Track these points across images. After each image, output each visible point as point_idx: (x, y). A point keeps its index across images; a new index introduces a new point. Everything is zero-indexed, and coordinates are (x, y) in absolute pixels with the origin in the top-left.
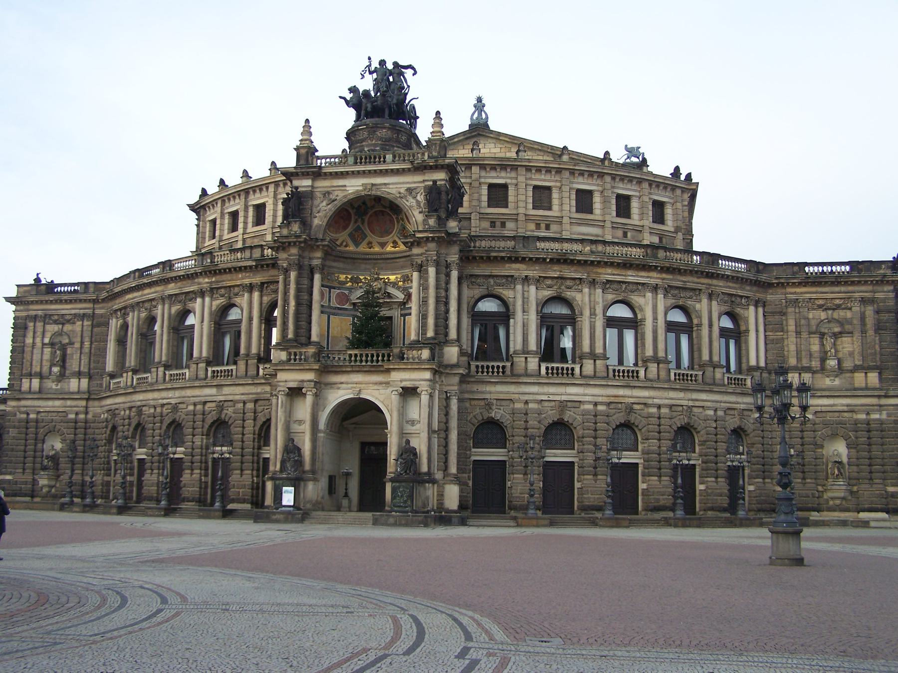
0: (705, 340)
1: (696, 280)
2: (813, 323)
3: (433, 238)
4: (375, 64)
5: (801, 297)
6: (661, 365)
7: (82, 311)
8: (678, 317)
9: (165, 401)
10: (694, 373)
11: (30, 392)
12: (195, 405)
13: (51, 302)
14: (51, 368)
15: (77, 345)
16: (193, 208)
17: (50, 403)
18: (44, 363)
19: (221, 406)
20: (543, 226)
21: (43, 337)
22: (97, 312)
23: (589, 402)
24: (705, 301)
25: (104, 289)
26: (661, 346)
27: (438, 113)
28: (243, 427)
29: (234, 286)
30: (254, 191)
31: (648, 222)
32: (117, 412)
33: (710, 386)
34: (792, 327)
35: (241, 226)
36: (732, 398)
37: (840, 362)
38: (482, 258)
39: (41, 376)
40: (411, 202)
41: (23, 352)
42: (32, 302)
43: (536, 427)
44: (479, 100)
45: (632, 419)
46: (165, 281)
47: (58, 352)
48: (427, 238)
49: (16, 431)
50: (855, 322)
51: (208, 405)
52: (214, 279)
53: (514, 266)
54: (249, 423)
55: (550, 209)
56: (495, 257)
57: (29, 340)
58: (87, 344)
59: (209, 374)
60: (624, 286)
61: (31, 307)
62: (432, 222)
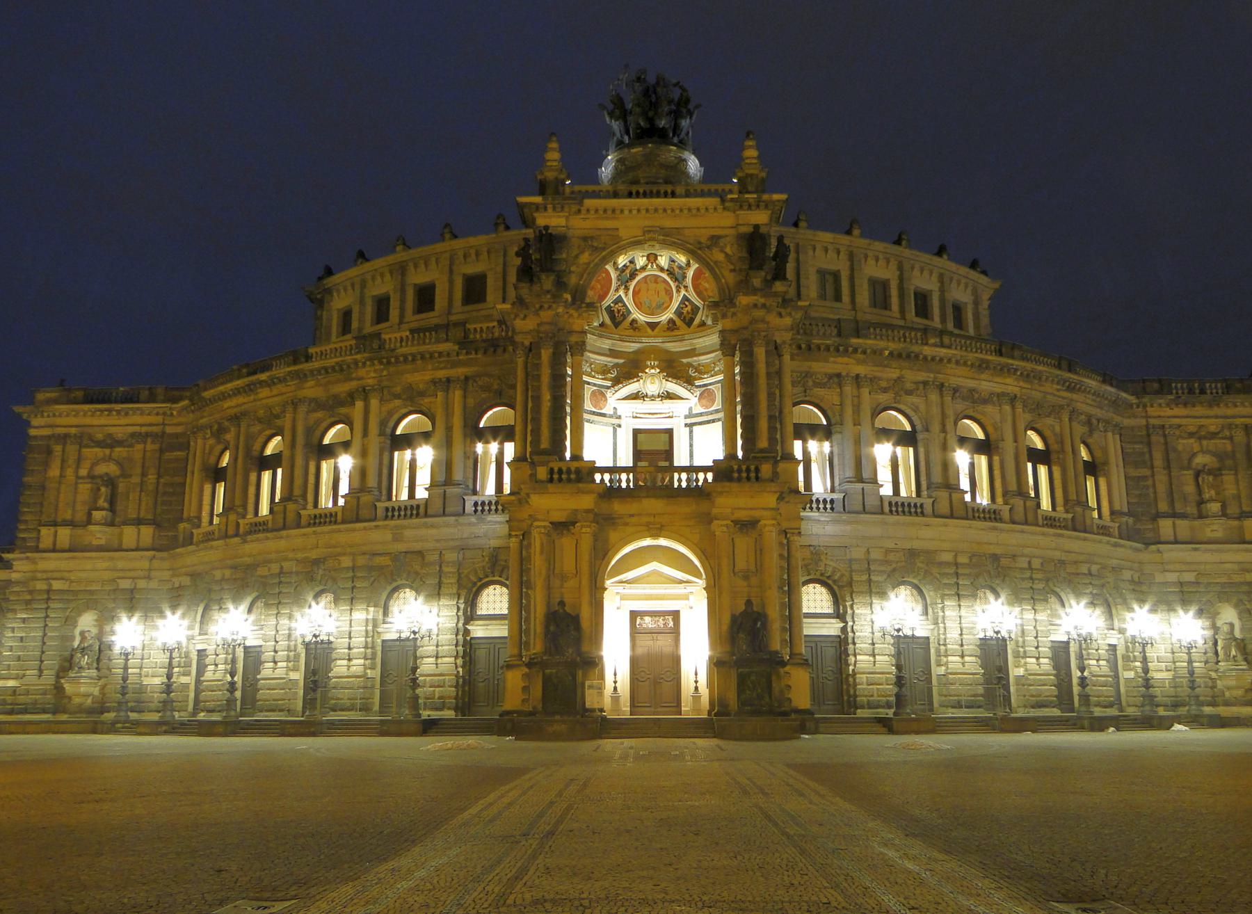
3: (764, 306)
6: (1029, 504)
7: (144, 429)
11: (54, 550)
14: (90, 515)
15: (136, 480)
18: (78, 507)
21: (78, 467)
22: (169, 430)
30: (416, 266)
34: (1158, 461)
35: (394, 314)
37: (1224, 507)
39: (71, 524)
40: (720, 257)
41: (43, 488)
47: (103, 489)
50: (1239, 456)
53: (840, 360)
57: (54, 472)
62: (757, 282)
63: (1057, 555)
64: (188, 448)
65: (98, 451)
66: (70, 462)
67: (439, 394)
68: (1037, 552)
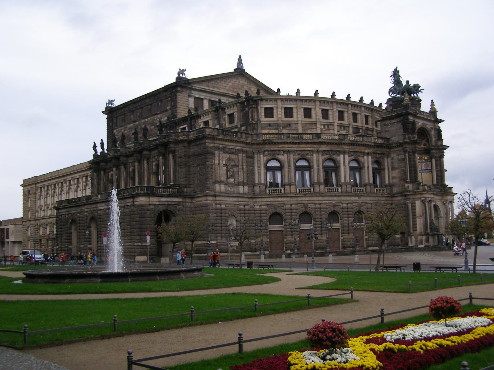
9: (327, 202)
15: (240, 167)
17: (231, 199)
19: (360, 205)
22: (248, 150)
25: (248, 138)
27: (432, 101)
29: (357, 152)
32: (279, 205)
42: (219, 139)
44: (240, 57)
47: (232, 170)
49: (215, 215)
52: (350, 147)
57: (217, 162)
61: (216, 142)
64: (253, 158)
66: (221, 158)
67: (366, 157)
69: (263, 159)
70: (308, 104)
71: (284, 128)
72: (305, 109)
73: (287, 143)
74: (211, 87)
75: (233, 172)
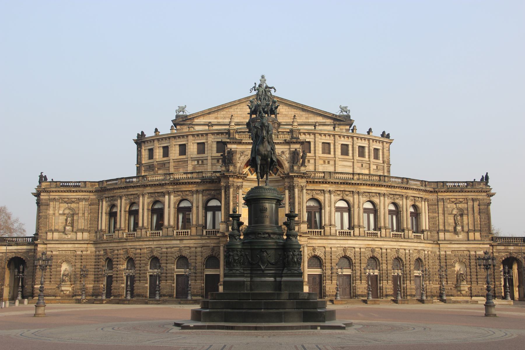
0: (405, 218)
1: (401, 191)
2: (450, 209)
4: (257, 86)
5: (444, 198)
7: (82, 197)
8: (392, 208)
9: (147, 246)
10: (400, 233)
11: (53, 240)
12: (167, 248)
13: (65, 192)
16: (136, 142)
17: (65, 246)
18: (60, 224)
20: (326, 162)
22: (91, 197)
23: (357, 247)
24: (405, 200)
26: (387, 221)
28: (196, 260)
29: (186, 191)
31: (372, 159)
33: (406, 239)
34: (441, 211)
36: (416, 245)
37: (463, 227)
38: (310, 182)
39: (57, 231)
42: (53, 191)
43: (335, 260)
44: (263, 77)
45: (375, 254)
46: (145, 186)
48: (295, 176)
50: (469, 209)
51: (175, 249)
52: (175, 187)
54: (199, 258)
55: (329, 153)
56: (317, 182)
57: (51, 212)
58: (86, 214)
59: (175, 233)
60: (371, 194)
61: (51, 194)
63: (397, 247)
65: (66, 205)
66: (56, 208)
67: (195, 196)
68: (389, 247)
69: (105, 206)
70: (182, 140)
71: (159, 169)
72: (180, 145)
73: (117, 189)
74: (221, 118)
75: (73, 220)
